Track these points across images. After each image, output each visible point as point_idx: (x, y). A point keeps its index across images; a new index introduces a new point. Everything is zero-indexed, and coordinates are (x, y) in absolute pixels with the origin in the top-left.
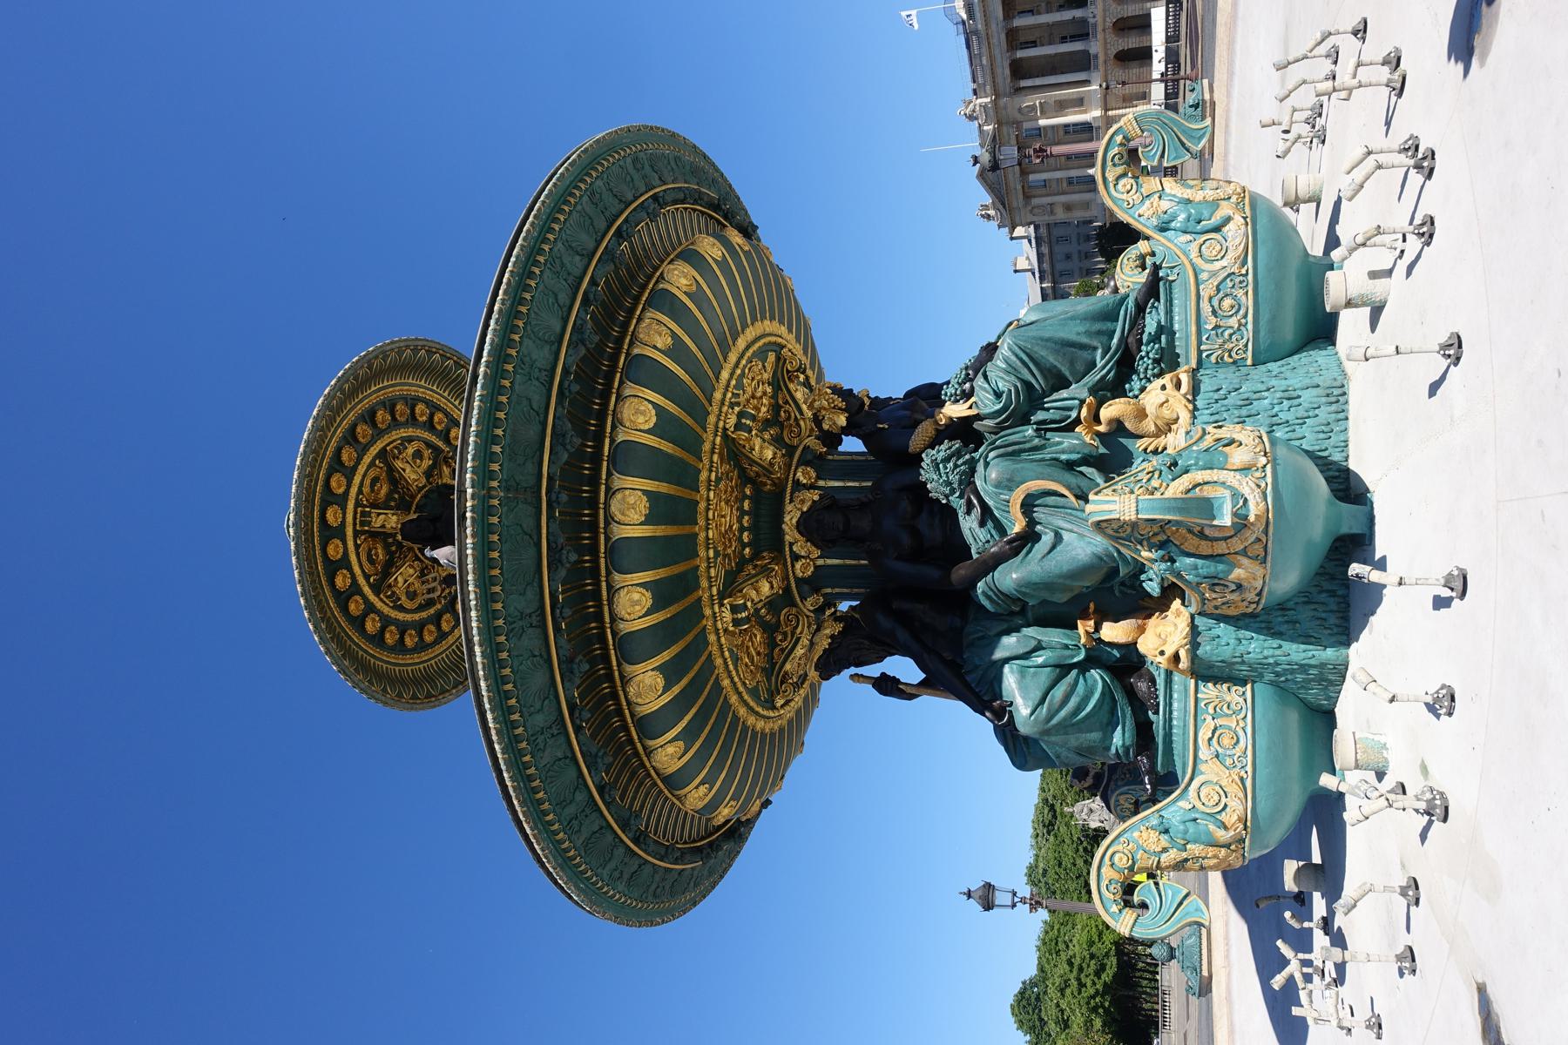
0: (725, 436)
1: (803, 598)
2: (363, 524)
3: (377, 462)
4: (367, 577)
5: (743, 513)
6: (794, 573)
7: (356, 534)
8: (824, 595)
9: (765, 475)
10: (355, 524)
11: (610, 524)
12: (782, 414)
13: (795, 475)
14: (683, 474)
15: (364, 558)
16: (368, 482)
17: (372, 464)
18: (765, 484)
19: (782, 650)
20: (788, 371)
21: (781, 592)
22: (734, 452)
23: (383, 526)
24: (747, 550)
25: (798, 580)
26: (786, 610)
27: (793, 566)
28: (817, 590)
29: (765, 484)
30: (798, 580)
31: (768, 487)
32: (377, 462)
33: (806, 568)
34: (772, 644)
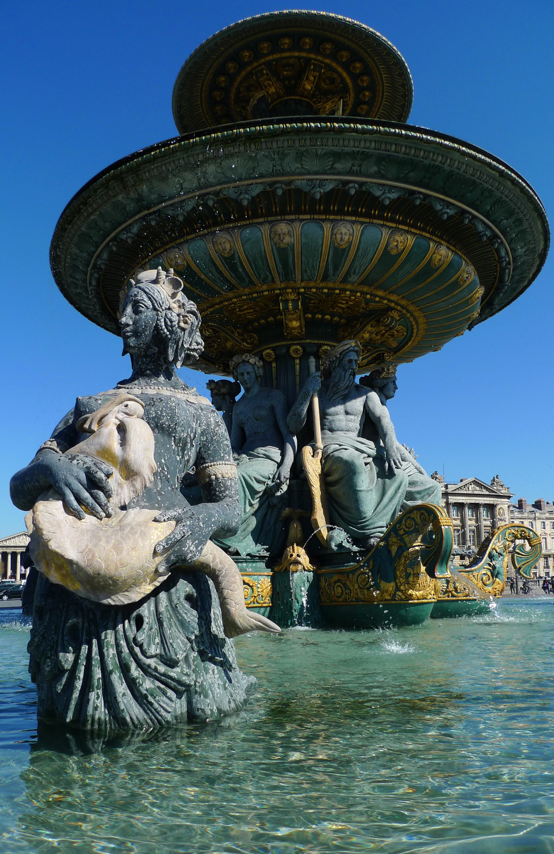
1: (274, 349)
2: (315, 65)
3: (341, 85)
4: (277, 60)
6: (294, 344)
7: (308, 61)
8: (270, 363)
10: (315, 60)
15: (291, 61)
16: (335, 75)
17: (343, 80)
19: (233, 332)
20: (384, 354)
23: (308, 79)
25: (289, 347)
28: (277, 359)
32: (341, 85)
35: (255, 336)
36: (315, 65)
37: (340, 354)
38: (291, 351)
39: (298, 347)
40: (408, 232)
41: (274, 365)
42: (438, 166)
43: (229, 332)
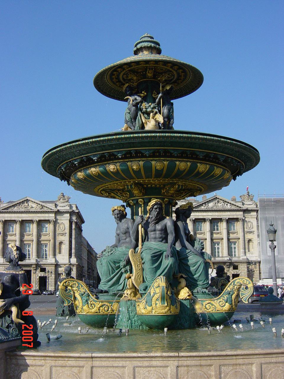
0: (177, 183)
1: (132, 200)
2: (149, 68)
5: (156, 185)
6: (140, 198)
9: (166, 191)
11: (155, 161)
12: (182, 191)
13: (166, 198)
14: (167, 176)
18: (163, 190)
19: (117, 193)
20: (194, 193)
21: (134, 195)
22: (173, 185)
24: (146, 186)
25: (138, 199)
26: (129, 194)
27: (141, 198)
29: (163, 190)
30: (138, 199)
31: (163, 191)
33: (141, 202)
34: (119, 190)
35: (128, 193)
36: (149, 68)
37: (152, 206)
38: (139, 202)
39: (141, 200)
40: (164, 160)
41: (134, 207)
42: (164, 141)
43: (115, 193)
